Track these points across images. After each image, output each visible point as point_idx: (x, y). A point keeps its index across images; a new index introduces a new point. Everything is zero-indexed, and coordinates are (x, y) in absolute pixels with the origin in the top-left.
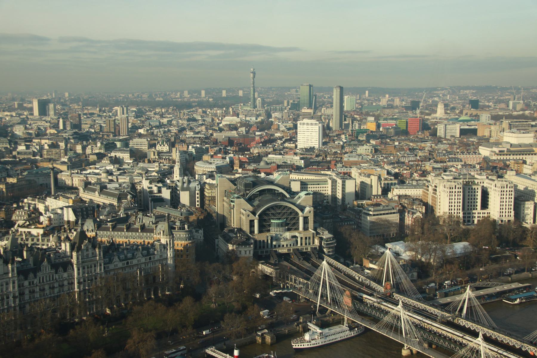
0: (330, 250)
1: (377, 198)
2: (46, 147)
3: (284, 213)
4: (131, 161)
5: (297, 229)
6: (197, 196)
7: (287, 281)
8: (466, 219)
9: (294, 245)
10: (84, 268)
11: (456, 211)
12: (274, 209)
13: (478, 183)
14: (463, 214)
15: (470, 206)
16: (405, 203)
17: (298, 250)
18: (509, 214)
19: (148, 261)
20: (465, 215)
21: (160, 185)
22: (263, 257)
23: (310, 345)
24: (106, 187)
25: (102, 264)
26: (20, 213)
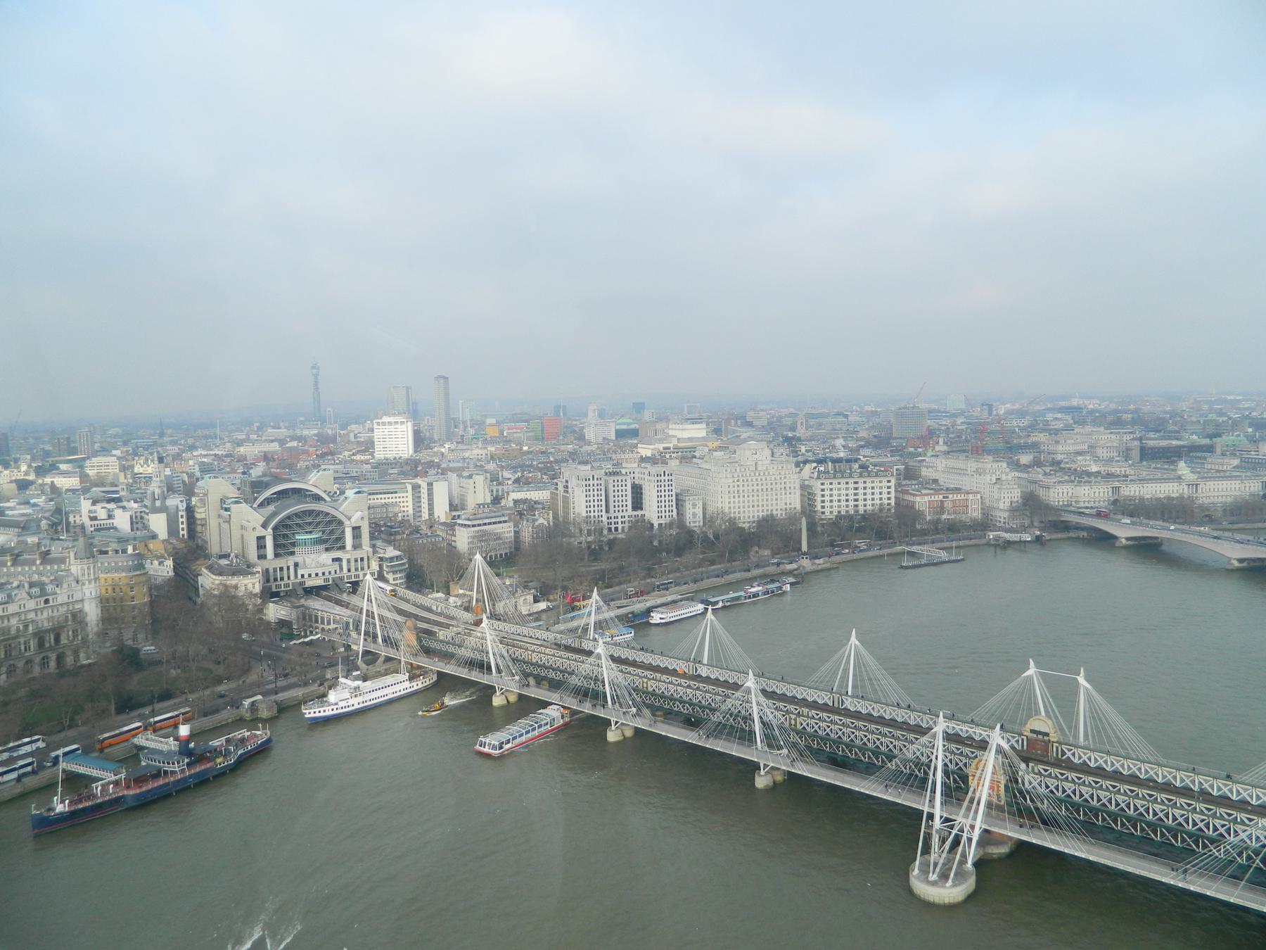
0: (395, 576)
1: (484, 507)
3: (318, 524)
5: (343, 548)
6: (181, 520)
7: (317, 625)
8: (613, 526)
11: (596, 514)
12: (300, 517)
13: (626, 473)
14: (608, 518)
15: (617, 506)
16: (523, 510)
17: (341, 579)
18: (671, 514)
20: (610, 521)
21: (112, 506)
22: (282, 594)
23: (337, 709)
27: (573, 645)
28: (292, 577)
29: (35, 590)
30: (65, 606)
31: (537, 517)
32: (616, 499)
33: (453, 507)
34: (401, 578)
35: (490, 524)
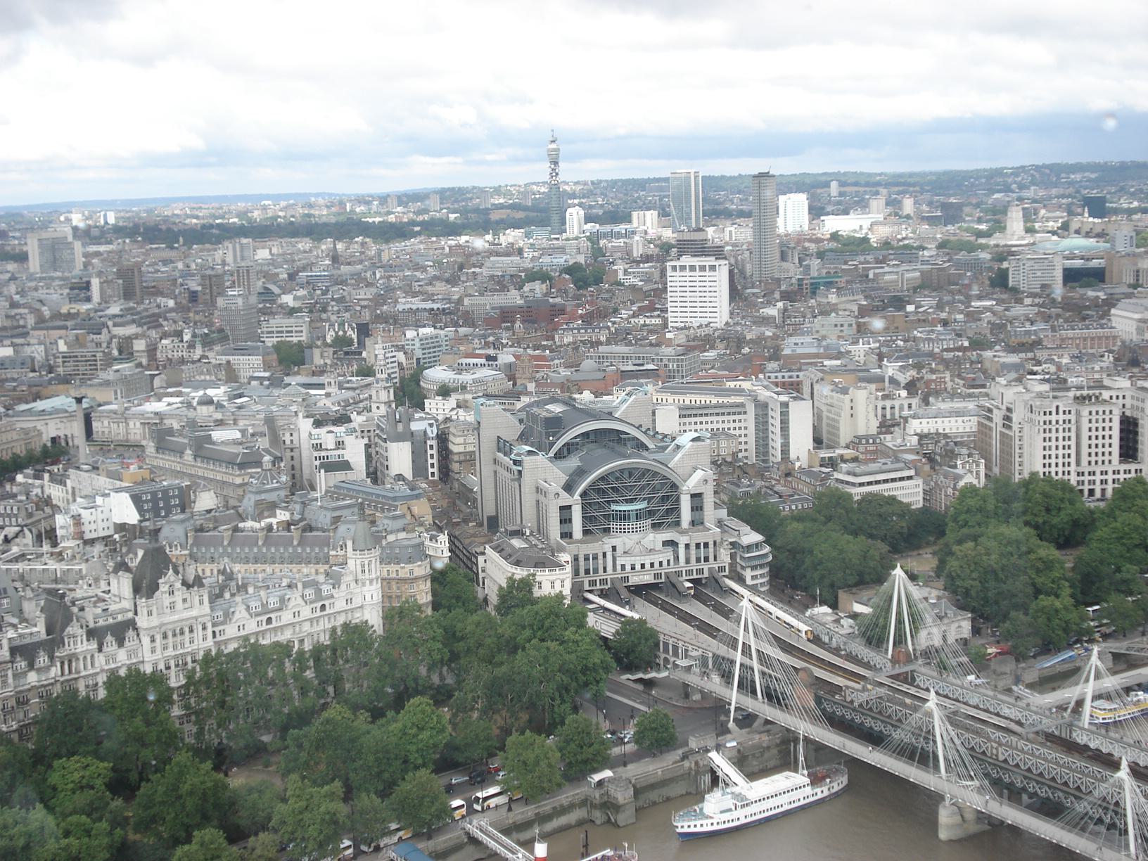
1: (867, 442)
2: (62, 347)
4: (267, 374)
5: (678, 523)
8: (1086, 488)
9: (668, 564)
10: (165, 636)
11: (1060, 469)
13: (1111, 398)
15: (1093, 454)
17: (679, 574)
19: (319, 613)
20: (1081, 478)
21: (340, 430)
24: (208, 439)
25: (209, 625)
26: (8, 508)
27: (1057, 733)
28: (609, 568)
29: (309, 591)
30: (344, 614)
31: (960, 471)
32: (1094, 442)
33: (818, 441)
34: (762, 576)
35: (886, 481)
